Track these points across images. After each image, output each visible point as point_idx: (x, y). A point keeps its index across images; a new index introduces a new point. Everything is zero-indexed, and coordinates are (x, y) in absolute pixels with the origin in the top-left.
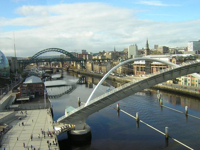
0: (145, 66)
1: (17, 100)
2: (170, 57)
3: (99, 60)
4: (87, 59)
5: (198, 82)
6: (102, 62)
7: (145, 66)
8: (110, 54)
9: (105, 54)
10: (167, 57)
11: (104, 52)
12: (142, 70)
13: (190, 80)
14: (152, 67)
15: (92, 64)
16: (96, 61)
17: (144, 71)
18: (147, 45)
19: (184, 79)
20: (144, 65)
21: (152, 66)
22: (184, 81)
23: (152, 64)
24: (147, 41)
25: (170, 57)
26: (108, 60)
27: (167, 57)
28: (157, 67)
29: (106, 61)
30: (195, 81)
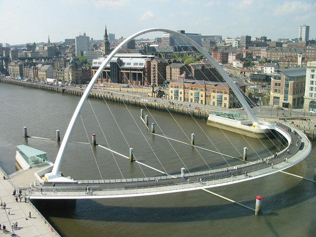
2: (146, 57)
3: (31, 59)
4: (11, 57)
6: (38, 64)
8: (46, 48)
9: (37, 48)
13: (183, 93)
15: (21, 66)
20: (108, 69)
22: (173, 94)
24: (106, 30)
25: (146, 57)
26: (45, 60)
27: (142, 57)
28: (129, 72)
29: (43, 61)
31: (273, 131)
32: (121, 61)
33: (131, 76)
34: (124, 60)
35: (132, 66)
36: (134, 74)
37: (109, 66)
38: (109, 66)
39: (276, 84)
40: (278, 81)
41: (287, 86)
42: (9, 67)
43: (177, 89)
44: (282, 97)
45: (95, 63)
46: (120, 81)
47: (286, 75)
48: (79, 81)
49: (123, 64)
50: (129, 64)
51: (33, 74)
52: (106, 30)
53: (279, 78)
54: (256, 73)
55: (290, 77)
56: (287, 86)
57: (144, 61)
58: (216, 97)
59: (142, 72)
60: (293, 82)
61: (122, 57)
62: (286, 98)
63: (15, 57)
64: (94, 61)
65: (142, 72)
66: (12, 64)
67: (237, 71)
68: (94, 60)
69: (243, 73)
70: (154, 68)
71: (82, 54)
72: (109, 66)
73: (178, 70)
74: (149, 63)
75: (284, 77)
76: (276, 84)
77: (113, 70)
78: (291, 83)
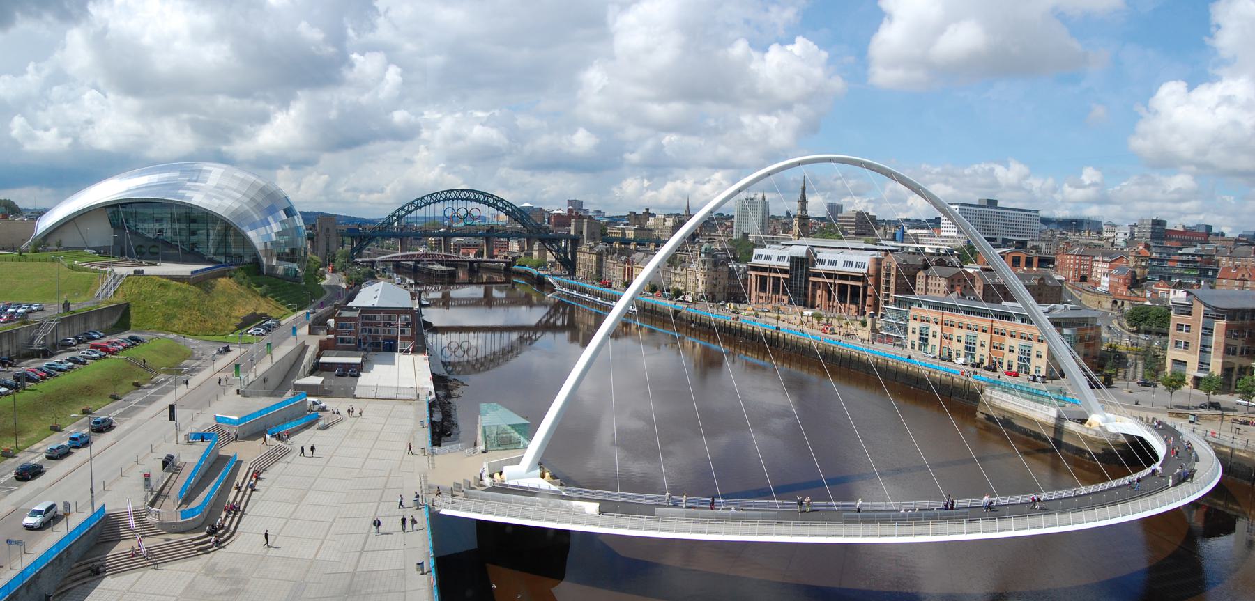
0: (787, 276)
1: (322, 360)
2: (876, 250)
3: (628, 242)
4: (585, 233)
5: (963, 341)
6: (637, 250)
7: (787, 276)
9: (651, 221)
10: (866, 249)
11: (648, 214)
12: (776, 291)
14: (814, 283)
15: (600, 255)
16: (616, 245)
17: (785, 293)
18: (803, 202)
19: (918, 331)
20: (785, 272)
21: (812, 279)
23: (812, 270)
24: (804, 189)
25: (876, 250)
27: (866, 249)
28: (832, 281)
30: (955, 339)
31: (1141, 439)
32: (816, 255)
33: (835, 295)
34: (823, 255)
35: (840, 268)
36: (843, 289)
37: (788, 264)
38: (786, 264)
39: (1180, 327)
40: (1184, 319)
41: (1207, 331)
42: (578, 255)
43: (925, 324)
44: (1192, 360)
45: (759, 257)
46: (805, 301)
47: (1206, 305)
48: (718, 297)
49: (822, 262)
50: (834, 263)
51: (621, 273)
52: (804, 189)
53: (1189, 314)
54: (1148, 303)
55: (1214, 309)
56: (1207, 331)
57: (867, 258)
58: (1016, 349)
59: (860, 284)
60: (1223, 323)
61: (819, 247)
62: (1203, 365)
63: (592, 237)
64: (757, 251)
65: (860, 284)
66: (584, 248)
67: (1103, 299)
68: (757, 251)
69: (1119, 303)
70: (888, 275)
71: (745, 235)
72: (786, 264)
73: (943, 282)
74: (878, 262)
75: (1199, 310)
76: (1180, 327)
77: (797, 275)
78: (1219, 325)
